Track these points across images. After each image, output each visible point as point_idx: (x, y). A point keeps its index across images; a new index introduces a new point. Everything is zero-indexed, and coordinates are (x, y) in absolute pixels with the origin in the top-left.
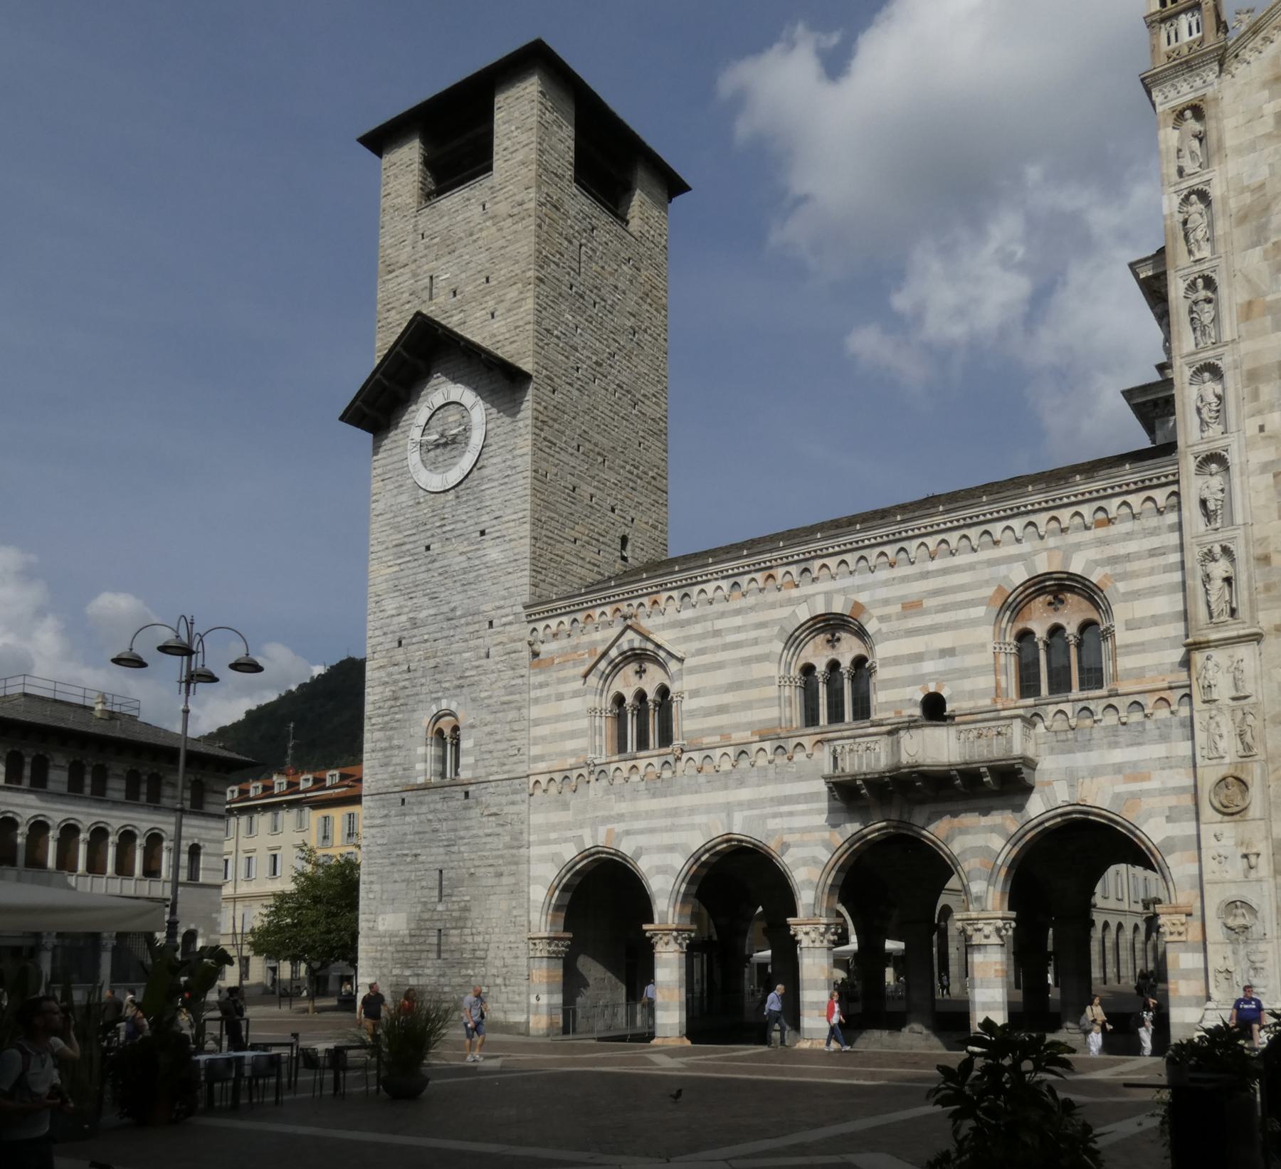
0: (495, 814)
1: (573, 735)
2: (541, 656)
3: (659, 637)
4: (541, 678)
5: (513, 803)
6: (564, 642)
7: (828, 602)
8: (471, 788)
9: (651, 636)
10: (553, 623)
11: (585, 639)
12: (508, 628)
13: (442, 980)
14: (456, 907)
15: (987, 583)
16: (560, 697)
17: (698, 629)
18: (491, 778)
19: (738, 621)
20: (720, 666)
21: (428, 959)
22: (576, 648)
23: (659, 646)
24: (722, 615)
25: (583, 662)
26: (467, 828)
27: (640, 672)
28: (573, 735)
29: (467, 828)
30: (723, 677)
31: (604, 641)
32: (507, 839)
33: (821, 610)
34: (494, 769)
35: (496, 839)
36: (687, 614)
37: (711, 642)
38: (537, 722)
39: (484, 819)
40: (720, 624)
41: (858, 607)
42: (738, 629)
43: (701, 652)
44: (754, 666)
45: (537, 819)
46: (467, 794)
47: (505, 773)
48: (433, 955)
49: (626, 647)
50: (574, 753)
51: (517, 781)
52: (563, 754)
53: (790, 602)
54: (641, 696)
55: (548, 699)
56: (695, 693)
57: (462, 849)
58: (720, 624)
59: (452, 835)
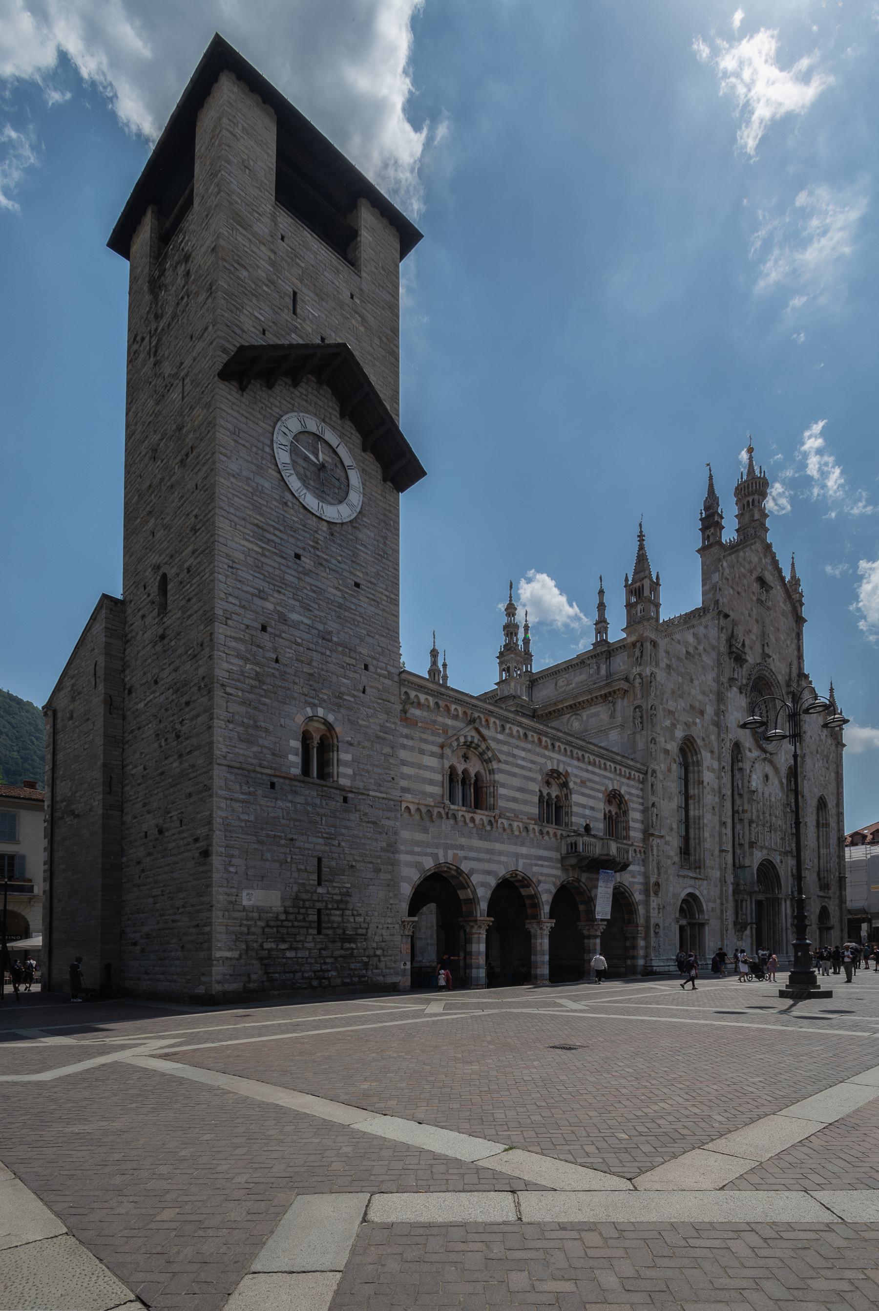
0: (374, 823)
1: (431, 782)
2: (408, 715)
3: (493, 745)
4: (406, 731)
5: (388, 818)
6: (425, 714)
7: (558, 766)
8: (350, 795)
9: (489, 741)
10: (423, 698)
11: (440, 719)
12: (382, 679)
13: (324, 952)
14: (337, 891)
15: (602, 784)
16: (422, 752)
17: (505, 748)
18: (371, 793)
19: (523, 754)
20: (514, 775)
21: (308, 934)
22: (434, 722)
23: (488, 748)
24: (517, 747)
25: (438, 735)
26: (347, 827)
27: (466, 758)
28: (431, 782)
29: (347, 827)
30: (517, 782)
31: (454, 728)
32: (384, 844)
33: (555, 768)
34: (374, 787)
35: (374, 843)
36: (500, 737)
37: (511, 759)
38: (404, 763)
39: (364, 824)
40: (516, 752)
41: (567, 774)
42: (523, 759)
43: (507, 763)
44: (530, 782)
45: (405, 834)
46: (345, 800)
47: (381, 792)
48: (315, 932)
49: (469, 739)
50: (431, 795)
51: (392, 803)
52: (424, 793)
53: (544, 756)
54: (465, 772)
55: (412, 749)
56: (503, 785)
57: (343, 844)
58: (516, 752)
59: (332, 830)
